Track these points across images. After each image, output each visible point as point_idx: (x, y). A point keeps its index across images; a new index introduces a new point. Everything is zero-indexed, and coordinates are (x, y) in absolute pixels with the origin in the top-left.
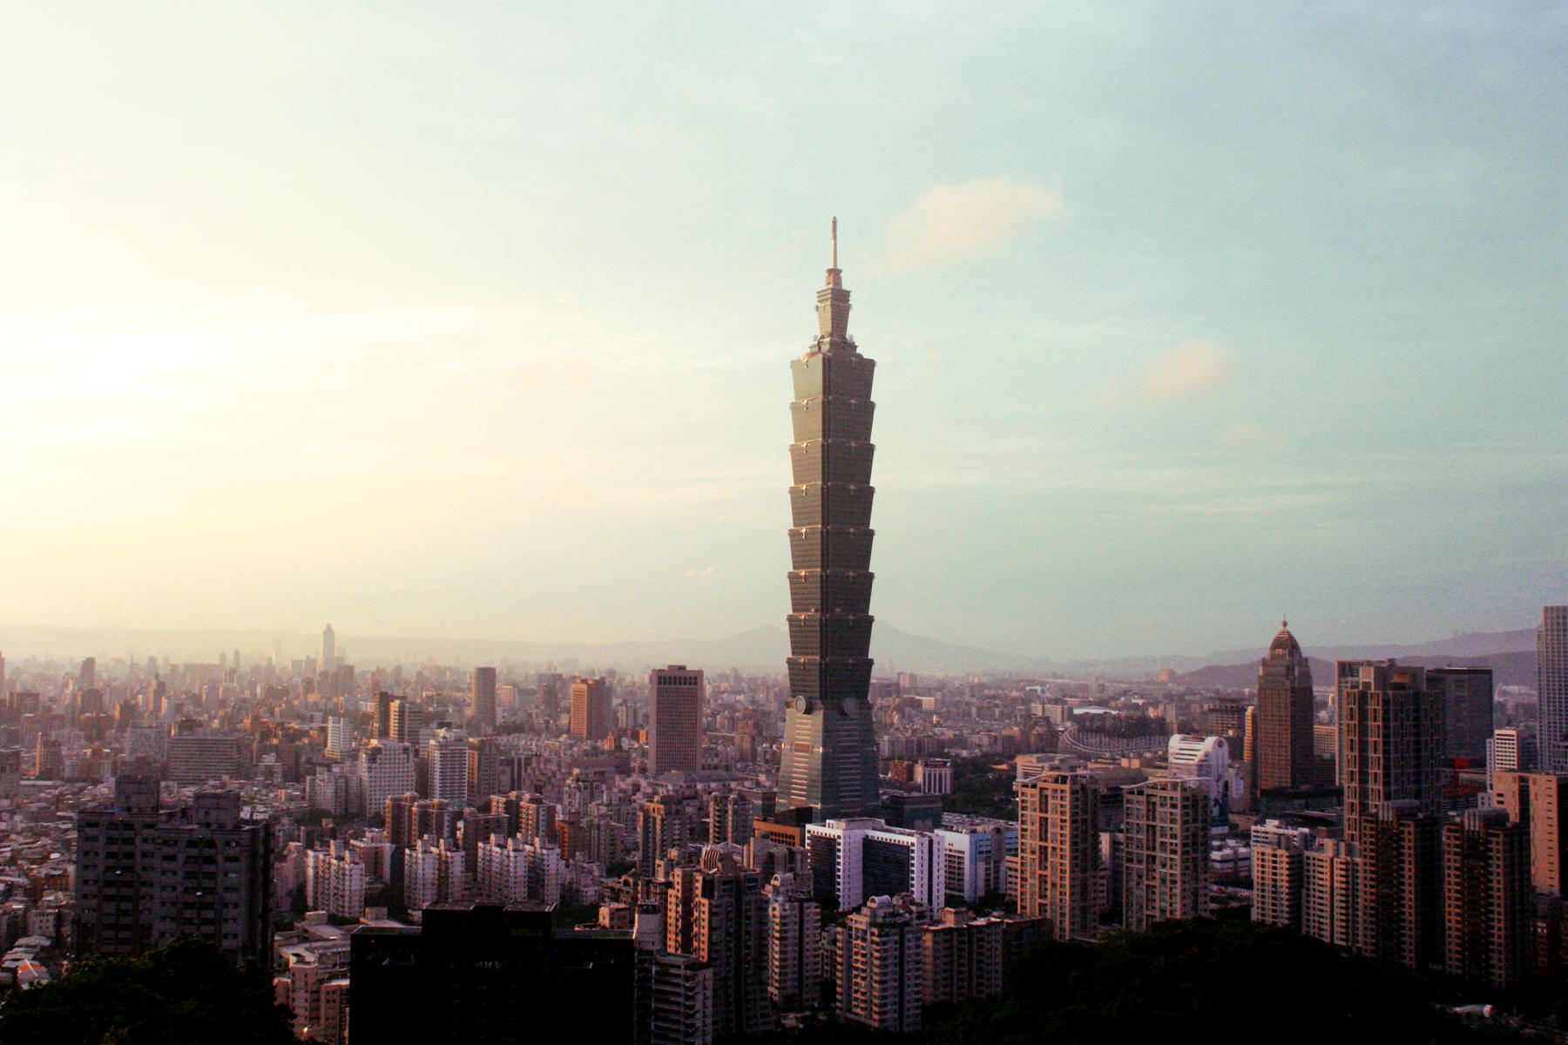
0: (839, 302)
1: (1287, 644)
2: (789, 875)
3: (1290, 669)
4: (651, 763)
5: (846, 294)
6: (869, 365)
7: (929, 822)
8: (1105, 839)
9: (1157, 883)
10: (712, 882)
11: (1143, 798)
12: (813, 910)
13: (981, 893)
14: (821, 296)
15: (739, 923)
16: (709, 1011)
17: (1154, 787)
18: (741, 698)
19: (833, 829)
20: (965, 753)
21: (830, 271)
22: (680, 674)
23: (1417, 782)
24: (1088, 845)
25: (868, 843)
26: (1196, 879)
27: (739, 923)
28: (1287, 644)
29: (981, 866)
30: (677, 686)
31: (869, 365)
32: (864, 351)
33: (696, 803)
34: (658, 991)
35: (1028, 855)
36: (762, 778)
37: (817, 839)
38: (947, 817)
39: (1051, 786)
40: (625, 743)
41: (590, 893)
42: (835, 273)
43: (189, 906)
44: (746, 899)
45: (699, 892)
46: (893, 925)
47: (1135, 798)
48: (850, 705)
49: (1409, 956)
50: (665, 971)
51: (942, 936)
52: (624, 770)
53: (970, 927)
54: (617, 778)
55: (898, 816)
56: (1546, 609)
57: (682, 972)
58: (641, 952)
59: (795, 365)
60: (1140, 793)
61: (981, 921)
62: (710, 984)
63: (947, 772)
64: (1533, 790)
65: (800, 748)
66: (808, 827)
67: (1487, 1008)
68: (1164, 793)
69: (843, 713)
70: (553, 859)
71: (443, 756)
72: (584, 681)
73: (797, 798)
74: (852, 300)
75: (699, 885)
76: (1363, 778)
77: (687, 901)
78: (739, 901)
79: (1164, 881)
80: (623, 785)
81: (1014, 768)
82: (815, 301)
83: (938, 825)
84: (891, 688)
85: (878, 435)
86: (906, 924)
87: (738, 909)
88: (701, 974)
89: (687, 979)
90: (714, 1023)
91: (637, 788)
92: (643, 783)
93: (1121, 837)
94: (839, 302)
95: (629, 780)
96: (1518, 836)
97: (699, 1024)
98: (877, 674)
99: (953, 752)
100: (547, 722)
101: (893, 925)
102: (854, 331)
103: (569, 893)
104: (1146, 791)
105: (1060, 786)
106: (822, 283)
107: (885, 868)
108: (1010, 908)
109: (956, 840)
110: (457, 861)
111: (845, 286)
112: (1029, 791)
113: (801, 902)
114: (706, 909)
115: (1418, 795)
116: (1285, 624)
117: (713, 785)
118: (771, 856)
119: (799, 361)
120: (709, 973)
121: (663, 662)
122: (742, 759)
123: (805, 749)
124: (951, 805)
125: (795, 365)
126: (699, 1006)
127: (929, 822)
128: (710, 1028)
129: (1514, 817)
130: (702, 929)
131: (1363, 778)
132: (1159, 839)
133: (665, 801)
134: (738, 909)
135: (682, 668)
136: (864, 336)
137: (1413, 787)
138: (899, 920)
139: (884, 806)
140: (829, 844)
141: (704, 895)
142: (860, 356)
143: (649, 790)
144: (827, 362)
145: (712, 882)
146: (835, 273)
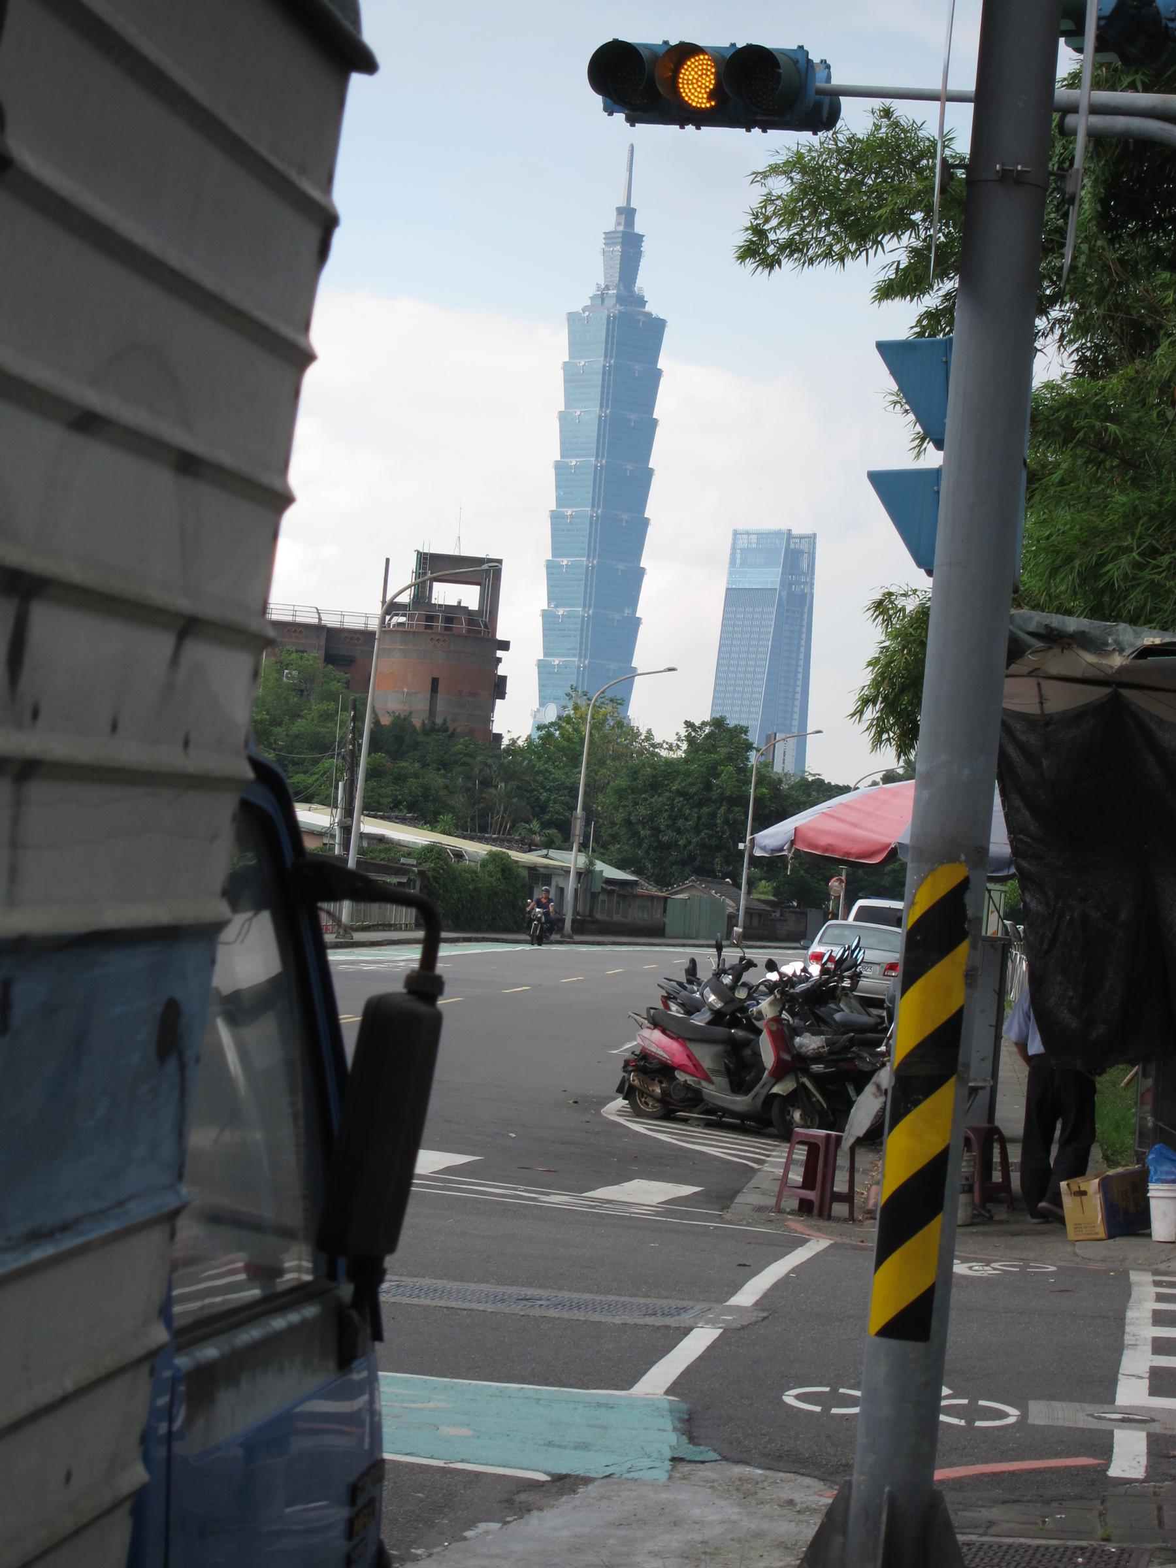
0: (628, 246)
5: (639, 238)
14: (609, 237)
21: (620, 211)
32: (654, 308)
42: (627, 214)
59: (572, 318)
74: (646, 247)
82: (600, 242)
85: (662, 408)
94: (628, 246)
102: (644, 282)
106: (610, 222)
111: (638, 229)
119: (576, 313)
125: (572, 318)
136: (655, 288)
142: (649, 315)
146: (627, 214)
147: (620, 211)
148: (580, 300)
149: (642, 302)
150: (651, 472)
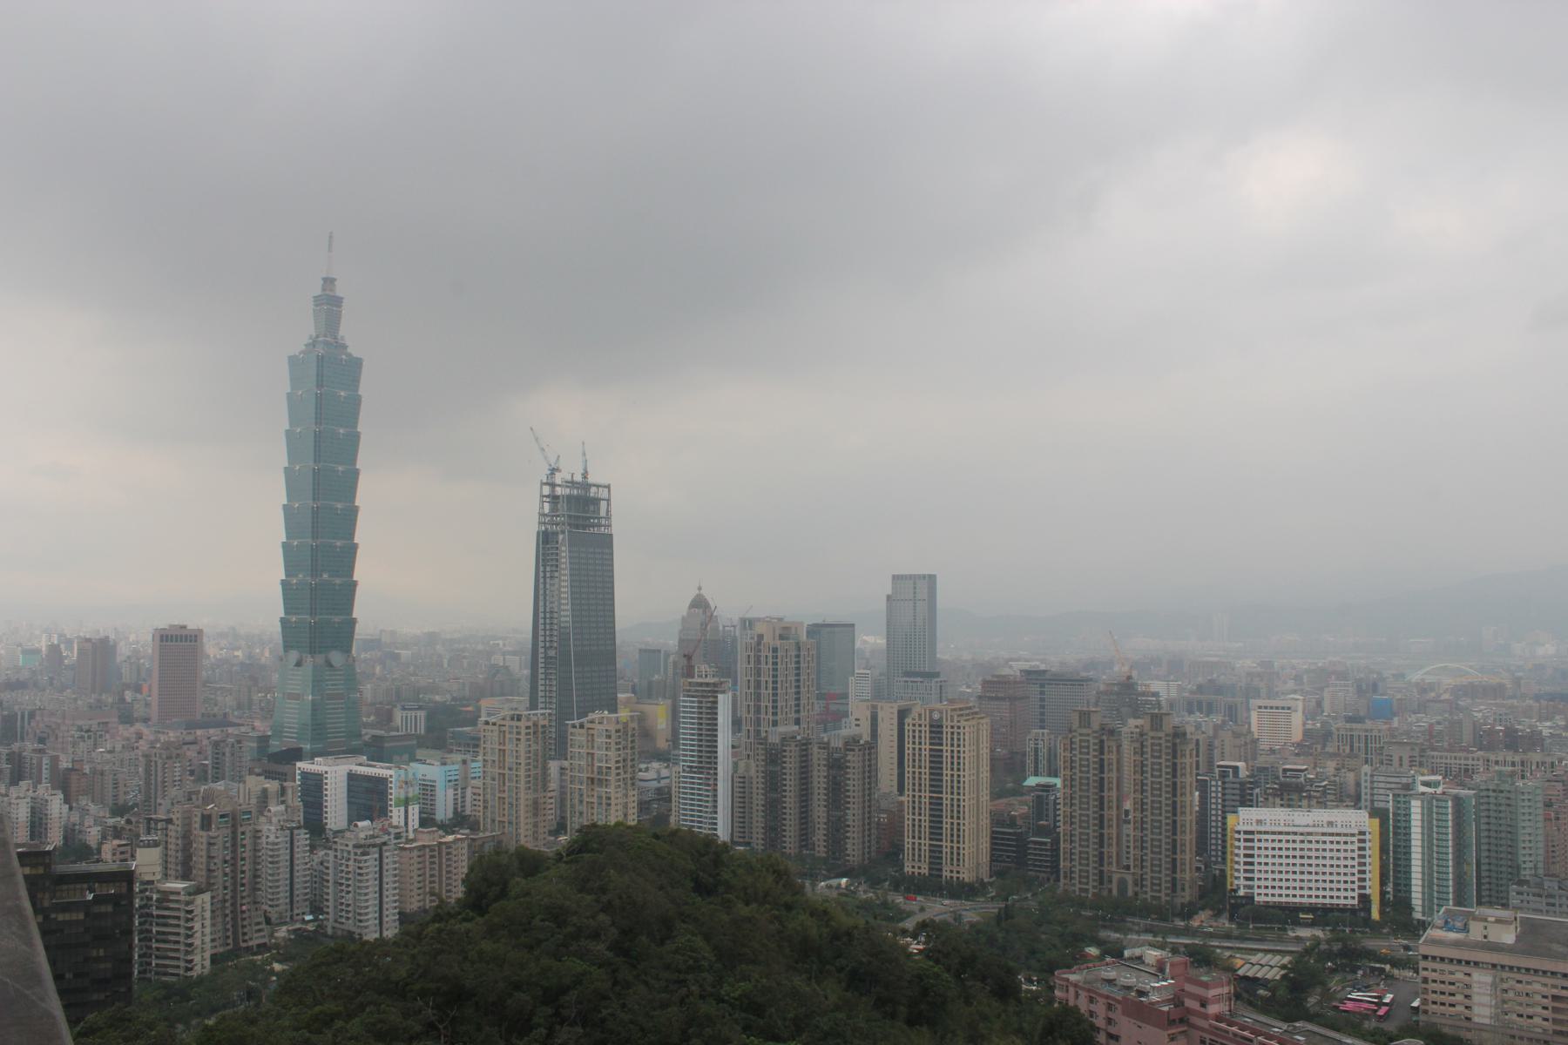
1: (700, 603)
2: (282, 807)
3: (704, 625)
4: (154, 712)
7: (406, 757)
8: (554, 766)
9: (595, 800)
10: (209, 816)
11: (583, 731)
12: (303, 837)
13: (450, 815)
14: (318, 300)
15: (234, 852)
16: (208, 930)
17: (592, 722)
18: (238, 653)
19: (317, 766)
20: (438, 698)
21: (325, 280)
22: (184, 633)
23: (798, 711)
24: (539, 771)
25: (352, 777)
26: (626, 796)
27: (234, 852)
28: (700, 603)
29: (451, 792)
30: (178, 644)
31: (356, 365)
32: (354, 350)
33: (197, 747)
34: (158, 916)
35: (489, 781)
36: (257, 723)
37: (306, 775)
38: (420, 753)
39: (508, 723)
40: (128, 696)
41: (93, 835)
42: (329, 282)
44: (240, 830)
45: (197, 826)
46: (374, 846)
47: (578, 730)
48: (337, 658)
49: (790, 842)
50: (165, 896)
51: (416, 853)
52: (127, 719)
54: (121, 727)
55: (377, 751)
56: (895, 578)
57: (182, 898)
58: (143, 883)
60: (582, 726)
61: (450, 838)
62: (208, 906)
63: (422, 714)
64: (880, 715)
65: (292, 696)
66: (299, 764)
67: (844, 881)
69: (329, 664)
70: (56, 807)
72: (88, 640)
73: (291, 742)
75: (198, 819)
76: (758, 711)
77: (187, 837)
78: (234, 832)
79: (600, 797)
80: (126, 734)
81: (479, 710)
83: (413, 759)
84: (373, 644)
86: (385, 844)
87: (234, 838)
88: (199, 899)
89: (188, 903)
90: (213, 940)
91: (139, 736)
92: (146, 731)
93: (566, 764)
95: (132, 730)
96: (871, 747)
97: (197, 942)
98: (362, 631)
99: (427, 697)
100: (51, 679)
101: (374, 846)
102: (346, 331)
103: (70, 833)
104: (587, 725)
105: (515, 723)
107: (368, 798)
108: (474, 826)
109: (431, 770)
111: (339, 293)
112: (490, 727)
113: (292, 830)
114: (204, 840)
115: (797, 722)
117: (212, 731)
118: (265, 791)
120: (207, 897)
121: (163, 624)
122: (239, 707)
123: (297, 697)
124: (422, 742)
125: (293, 361)
126: (197, 926)
127: (406, 757)
128: (208, 945)
129: (866, 737)
130: (200, 859)
131: (758, 711)
132: (597, 764)
133: (167, 746)
134: (234, 838)
135: (184, 627)
136: (355, 336)
137: (794, 715)
138: (378, 841)
139: (366, 744)
141: (202, 828)
143: (152, 738)
144: (320, 360)
145: (209, 816)
146: (329, 282)
147: (325, 280)
148: (298, 345)
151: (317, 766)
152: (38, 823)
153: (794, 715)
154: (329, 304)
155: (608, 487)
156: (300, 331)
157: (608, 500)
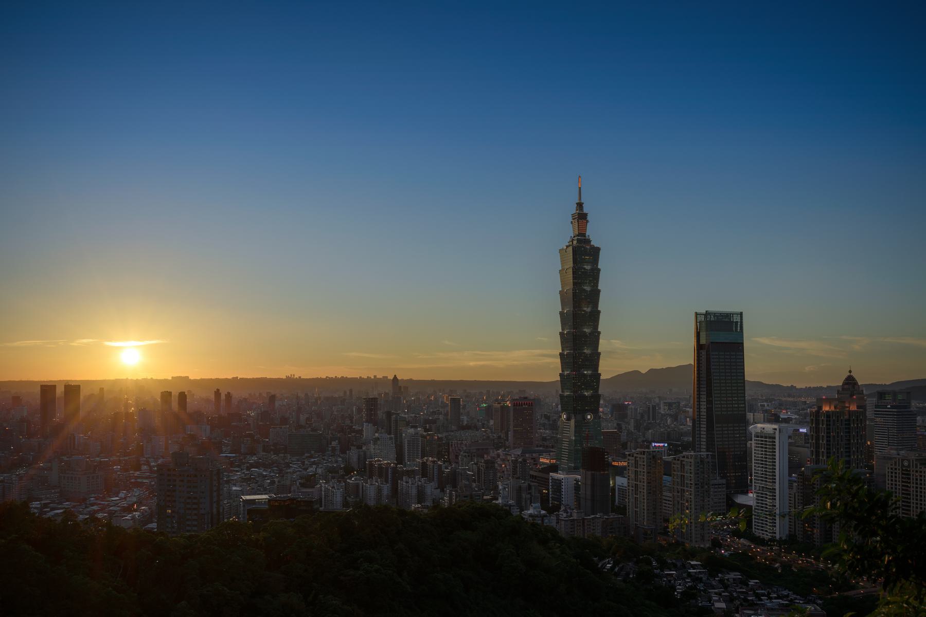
6: (597, 251)
21: (577, 204)
23: (849, 456)
31: (597, 251)
32: (595, 243)
42: (580, 205)
43: (189, 498)
53: (584, 519)
68: (689, 460)
71: (409, 441)
91: (498, 455)
94: (581, 217)
102: (590, 232)
106: (573, 210)
110: (386, 489)
111: (585, 211)
116: (850, 372)
140: (558, 483)
146: (580, 205)
147: (577, 204)
149: (589, 241)
150: (599, 312)
151: (559, 476)
152: (421, 497)
153: (847, 459)
154: (581, 217)
155: (741, 314)
156: (566, 233)
157: (741, 322)
